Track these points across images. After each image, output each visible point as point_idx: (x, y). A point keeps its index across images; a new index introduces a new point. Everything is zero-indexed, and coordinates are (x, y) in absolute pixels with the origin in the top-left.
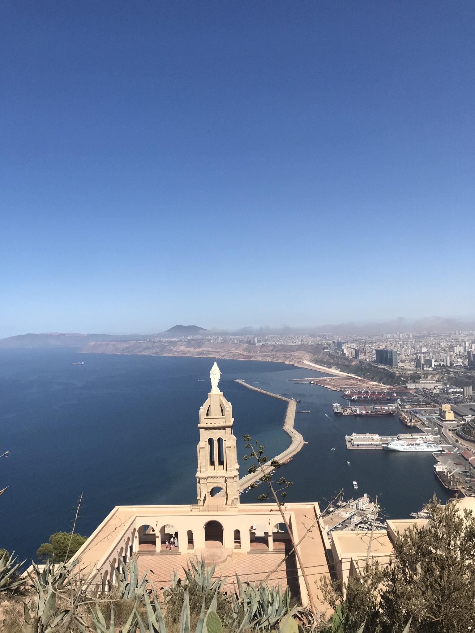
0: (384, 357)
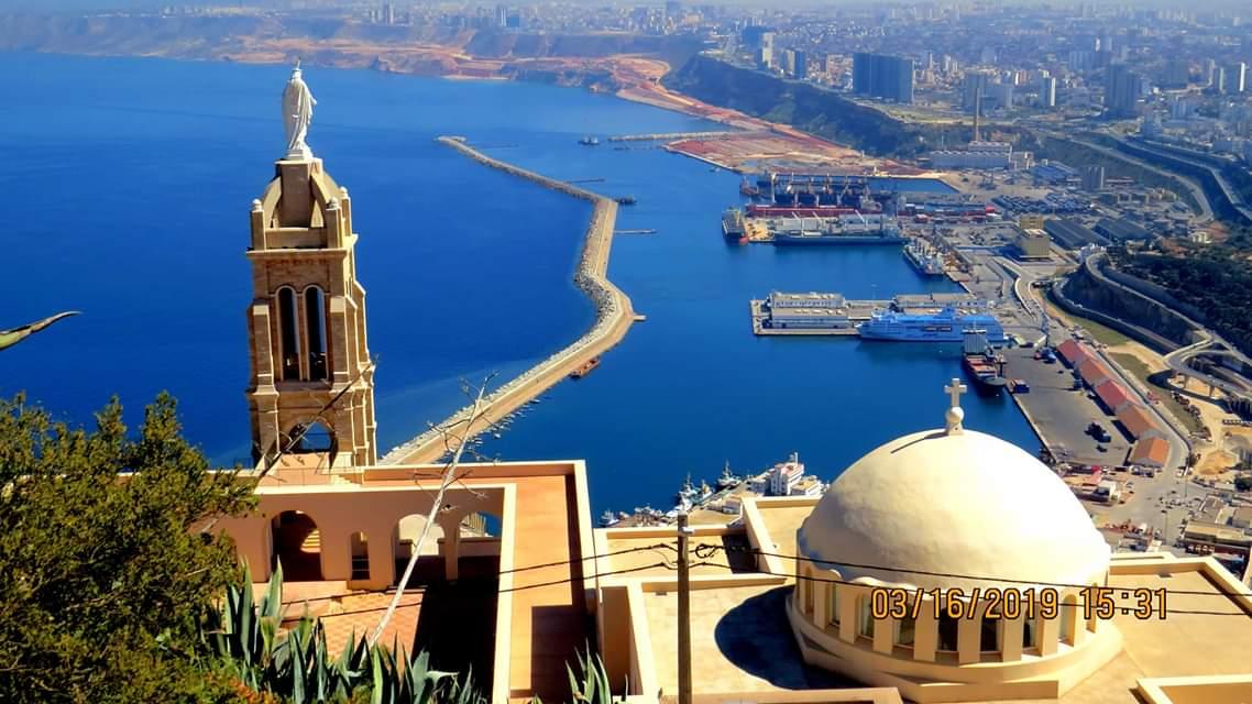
0: (880, 73)
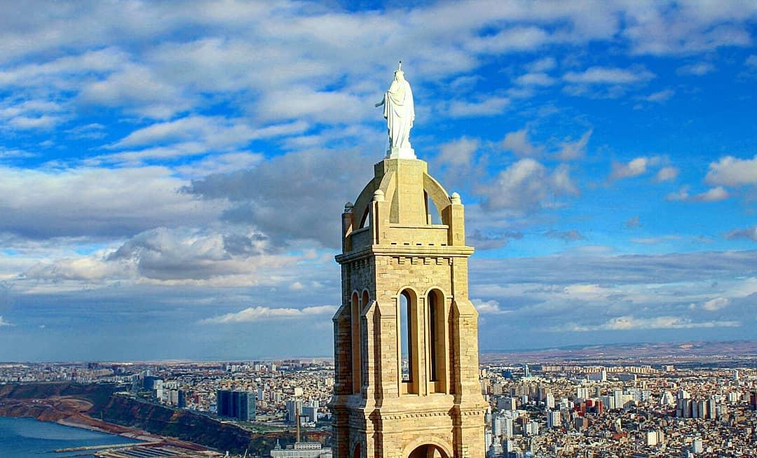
0: (231, 403)
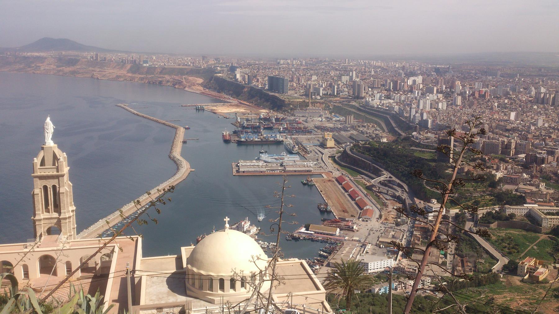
0: (276, 83)
